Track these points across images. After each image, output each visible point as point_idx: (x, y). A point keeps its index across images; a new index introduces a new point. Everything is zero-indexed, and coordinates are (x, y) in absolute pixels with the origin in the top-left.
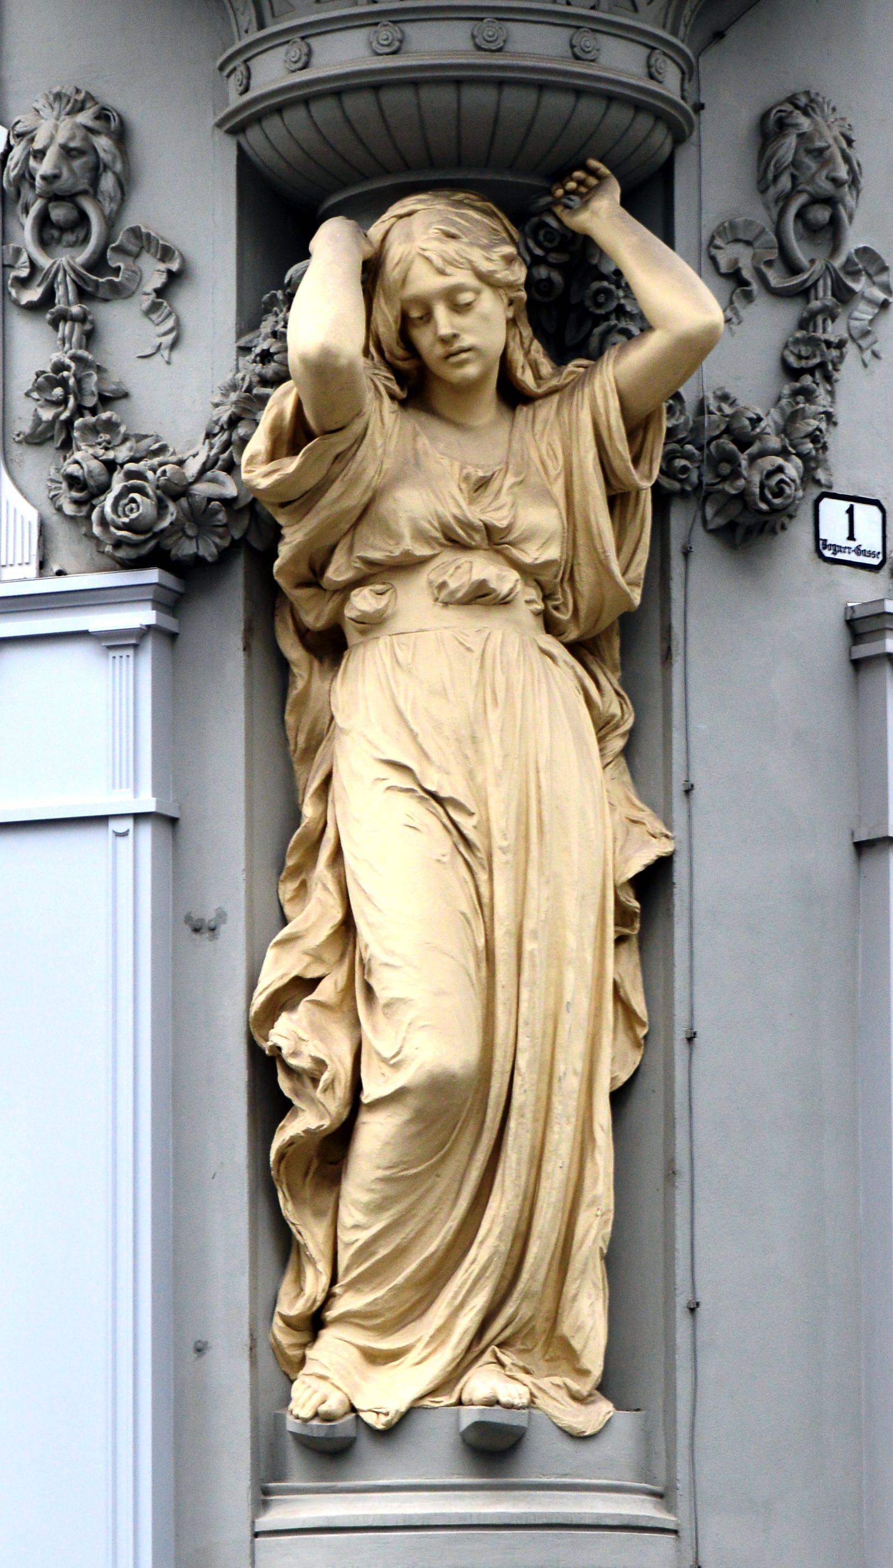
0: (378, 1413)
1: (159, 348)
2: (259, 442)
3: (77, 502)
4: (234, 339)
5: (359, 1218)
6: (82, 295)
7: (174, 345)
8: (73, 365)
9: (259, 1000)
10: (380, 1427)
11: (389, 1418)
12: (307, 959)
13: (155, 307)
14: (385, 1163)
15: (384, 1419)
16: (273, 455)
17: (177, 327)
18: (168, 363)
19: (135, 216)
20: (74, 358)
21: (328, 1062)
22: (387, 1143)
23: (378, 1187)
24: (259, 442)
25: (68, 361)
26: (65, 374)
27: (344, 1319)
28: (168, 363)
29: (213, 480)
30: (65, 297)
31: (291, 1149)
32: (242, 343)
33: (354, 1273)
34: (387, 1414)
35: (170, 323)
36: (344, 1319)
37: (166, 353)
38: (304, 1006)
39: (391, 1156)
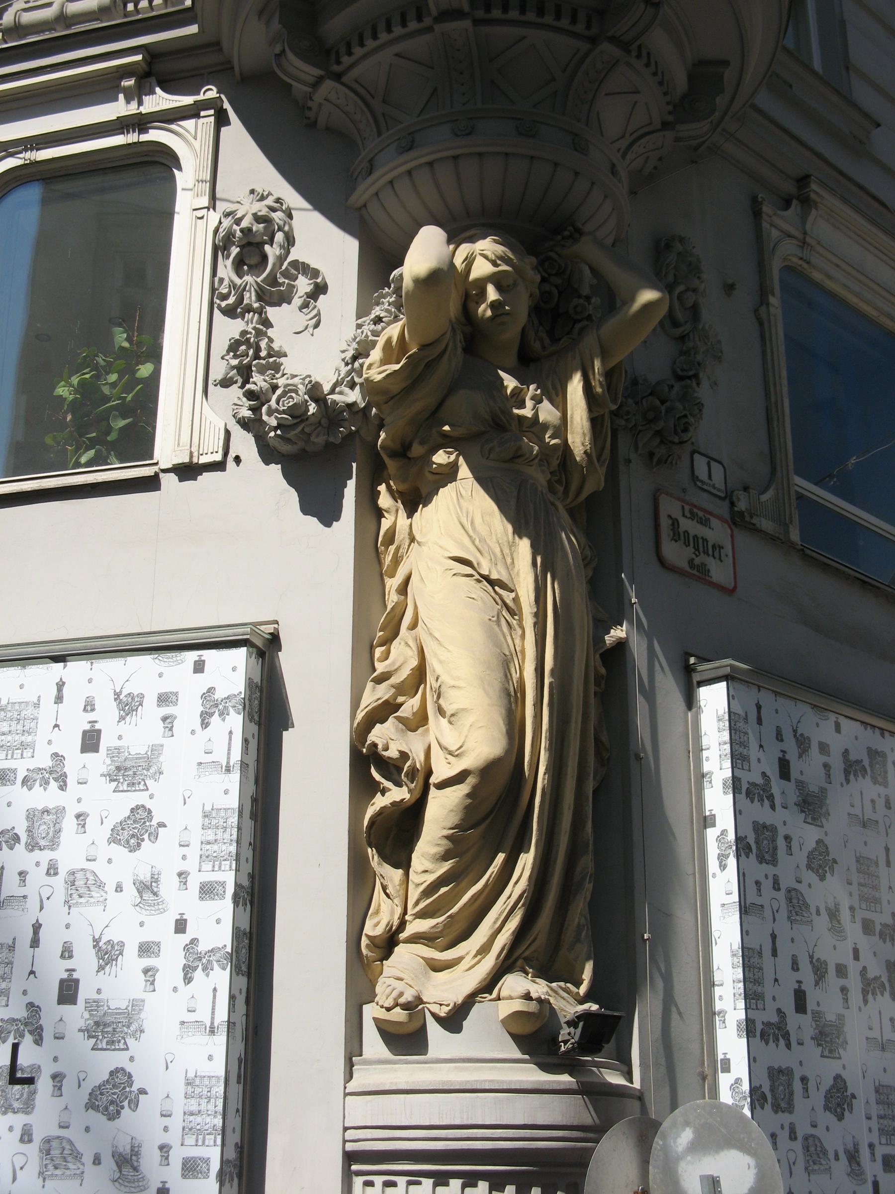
0: (441, 1005)
1: (306, 328)
2: (376, 354)
3: (251, 409)
4: (355, 318)
5: (428, 865)
6: (259, 298)
7: (317, 326)
8: (253, 332)
9: (360, 715)
10: (443, 1015)
11: (450, 1008)
12: (393, 690)
13: (305, 305)
14: (450, 825)
15: (446, 1009)
16: (385, 361)
17: (318, 314)
18: (312, 335)
19: (295, 254)
20: (254, 328)
21: (410, 754)
22: (452, 811)
23: (445, 842)
24: (376, 354)
25: (250, 330)
26: (248, 336)
27: (415, 939)
28: (312, 335)
29: (341, 393)
30: (249, 297)
31: (379, 818)
32: (359, 321)
33: (422, 905)
34: (448, 1005)
35: (315, 312)
36: (415, 939)
37: (311, 329)
38: (391, 719)
39: (455, 819)
